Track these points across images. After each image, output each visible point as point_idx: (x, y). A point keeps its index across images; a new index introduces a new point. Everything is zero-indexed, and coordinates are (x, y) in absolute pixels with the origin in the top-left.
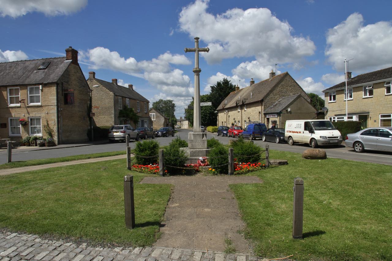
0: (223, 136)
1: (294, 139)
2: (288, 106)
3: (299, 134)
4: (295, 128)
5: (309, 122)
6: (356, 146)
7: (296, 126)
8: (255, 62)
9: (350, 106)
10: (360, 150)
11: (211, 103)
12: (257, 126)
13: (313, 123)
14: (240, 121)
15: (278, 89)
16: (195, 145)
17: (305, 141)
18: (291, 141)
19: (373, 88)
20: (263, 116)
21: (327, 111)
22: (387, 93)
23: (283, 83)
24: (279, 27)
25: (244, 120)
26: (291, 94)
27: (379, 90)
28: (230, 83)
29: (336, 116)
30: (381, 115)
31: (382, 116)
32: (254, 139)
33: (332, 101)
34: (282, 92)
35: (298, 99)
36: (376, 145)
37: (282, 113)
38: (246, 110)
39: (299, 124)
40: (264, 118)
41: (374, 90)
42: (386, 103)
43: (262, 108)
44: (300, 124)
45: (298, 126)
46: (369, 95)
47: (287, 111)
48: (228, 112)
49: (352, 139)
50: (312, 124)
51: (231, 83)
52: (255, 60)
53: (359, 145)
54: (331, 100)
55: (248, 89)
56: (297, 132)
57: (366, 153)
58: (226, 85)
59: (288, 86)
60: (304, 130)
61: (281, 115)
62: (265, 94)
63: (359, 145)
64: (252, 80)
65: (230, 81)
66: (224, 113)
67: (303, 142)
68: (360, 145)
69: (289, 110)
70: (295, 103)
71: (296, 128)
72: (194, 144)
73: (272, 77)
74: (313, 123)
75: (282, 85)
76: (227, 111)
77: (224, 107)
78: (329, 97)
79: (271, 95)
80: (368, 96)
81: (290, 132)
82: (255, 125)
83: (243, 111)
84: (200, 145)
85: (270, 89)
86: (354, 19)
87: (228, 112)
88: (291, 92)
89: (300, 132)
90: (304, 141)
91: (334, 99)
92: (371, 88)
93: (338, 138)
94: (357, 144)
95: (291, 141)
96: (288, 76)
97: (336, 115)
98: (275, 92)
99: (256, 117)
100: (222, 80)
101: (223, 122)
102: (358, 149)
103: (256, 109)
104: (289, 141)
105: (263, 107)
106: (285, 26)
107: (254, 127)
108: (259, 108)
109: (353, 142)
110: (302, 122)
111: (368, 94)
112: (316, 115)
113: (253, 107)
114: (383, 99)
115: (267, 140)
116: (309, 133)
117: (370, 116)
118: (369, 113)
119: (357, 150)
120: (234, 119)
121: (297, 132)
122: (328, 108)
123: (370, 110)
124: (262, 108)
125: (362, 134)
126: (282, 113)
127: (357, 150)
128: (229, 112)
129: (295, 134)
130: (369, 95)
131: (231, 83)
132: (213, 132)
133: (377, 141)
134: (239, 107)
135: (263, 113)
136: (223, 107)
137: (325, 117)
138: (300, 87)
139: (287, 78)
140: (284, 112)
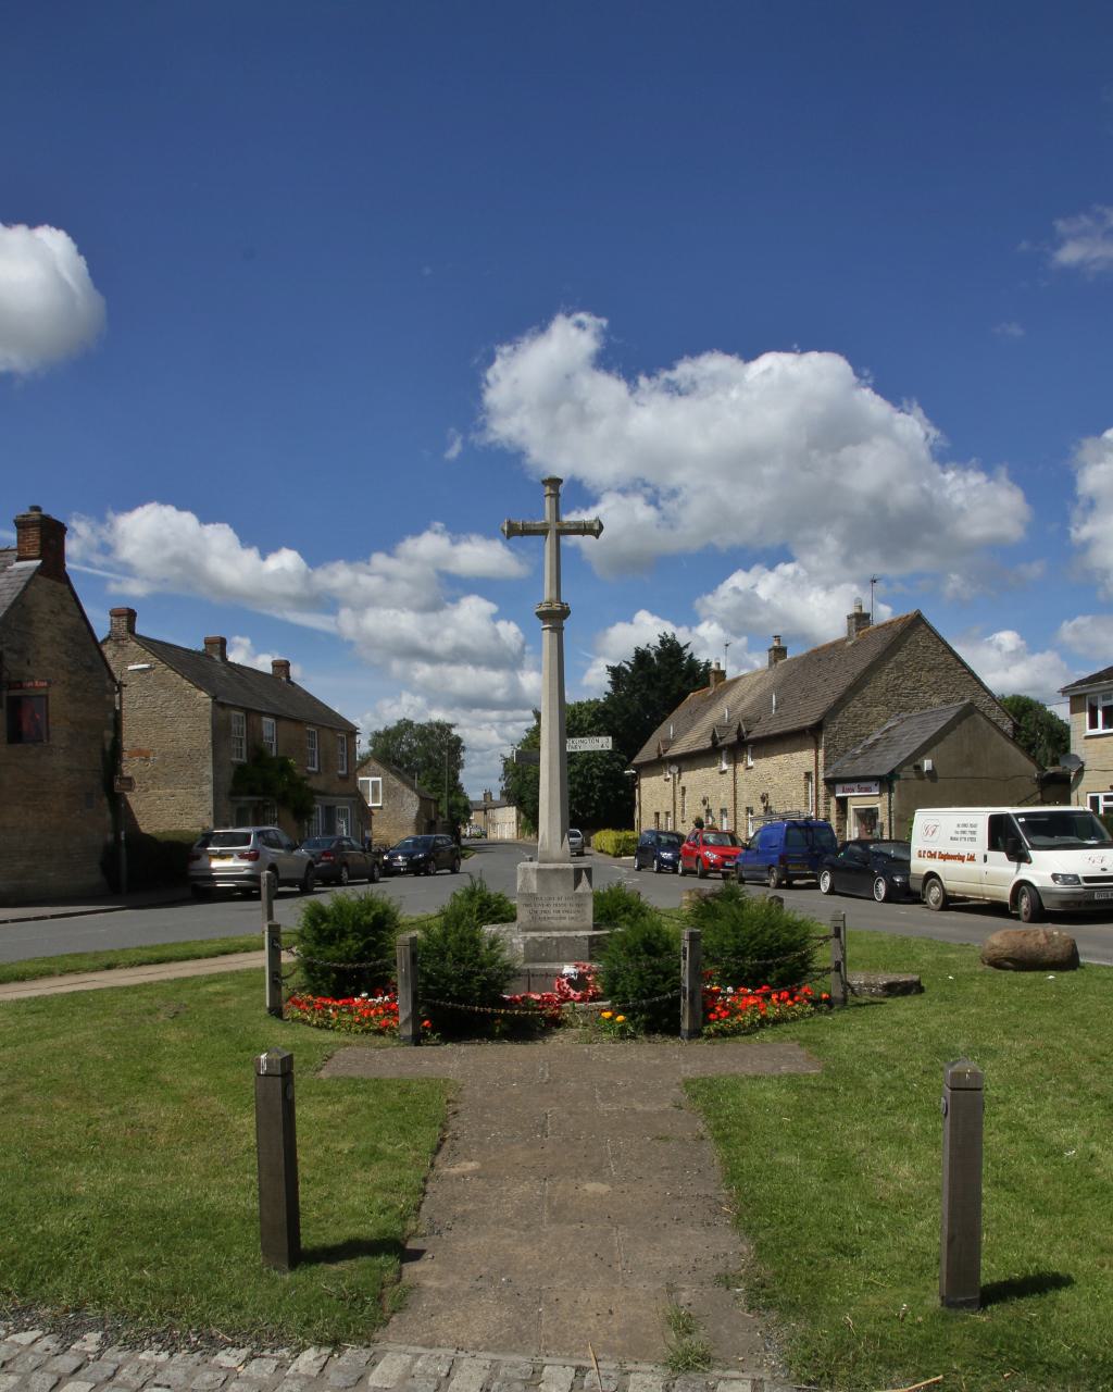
0: (659, 871)
1: (949, 885)
2: (924, 750)
3: (967, 865)
5: (1008, 815)
7: (957, 832)
8: (788, 569)
11: (610, 738)
12: (797, 833)
13: (1022, 820)
14: (730, 812)
15: (883, 679)
16: (543, 915)
17: (991, 893)
18: (935, 893)
20: (822, 789)
21: (1081, 772)
23: (901, 656)
24: (886, 430)
25: (744, 806)
26: (935, 700)
28: (687, 652)
32: (784, 882)
35: (964, 722)
37: (898, 777)
38: (751, 763)
39: (965, 825)
40: (827, 797)
43: (817, 757)
45: (964, 832)
47: (918, 768)
48: (680, 772)
50: (1021, 824)
51: (691, 655)
52: (789, 559)
54: (1093, 724)
55: (760, 681)
56: (961, 858)
58: (672, 660)
59: (921, 669)
60: (989, 849)
61: (895, 785)
62: (831, 700)
64: (776, 644)
65: (686, 646)
66: (662, 777)
67: (983, 895)
69: (927, 764)
70: (953, 735)
71: (955, 839)
73: (858, 630)
74: (1022, 820)
75: (899, 666)
76: (674, 769)
77: (665, 751)
78: (1087, 714)
79: (855, 706)
81: (932, 855)
82: (788, 828)
83: (741, 767)
84: (567, 915)
85: (849, 680)
87: (680, 772)
88: (936, 692)
89: (972, 858)
90: (986, 892)
95: (935, 893)
96: (922, 627)
98: (867, 691)
99: (794, 794)
100: (656, 642)
101: (657, 814)
104: (930, 891)
105: (821, 753)
106: (912, 426)
107: (787, 835)
108: (804, 759)
110: (978, 818)
112: (1036, 788)
113: (779, 754)
116: (1010, 859)
120: (704, 802)
121: (961, 858)
122: (1082, 759)
124: (817, 757)
126: (898, 777)
128: (684, 774)
129: (950, 863)
131: (691, 655)
132: (620, 856)
134: (724, 753)
135: (821, 776)
136: (659, 750)
137: (1073, 796)
138: (971, 673)
139: (918, 636)
140: (908, 772)
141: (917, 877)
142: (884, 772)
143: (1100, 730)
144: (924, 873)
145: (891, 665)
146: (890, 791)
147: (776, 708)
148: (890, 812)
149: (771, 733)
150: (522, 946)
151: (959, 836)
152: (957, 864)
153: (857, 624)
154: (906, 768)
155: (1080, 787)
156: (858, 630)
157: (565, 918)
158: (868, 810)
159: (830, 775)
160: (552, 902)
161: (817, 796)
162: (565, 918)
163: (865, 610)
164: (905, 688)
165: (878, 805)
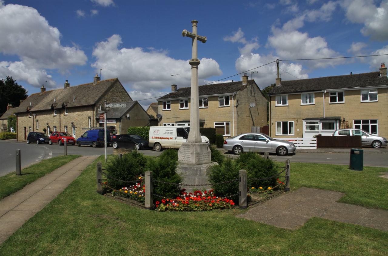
0: (39, 143)
1: (163, 145)
5: (183, 128)
6: (236, 149)
7: (166, 132)
8: (18, 63)
12: (101, 132)
13: (186, 129)
14: (32, 127)
15: (110, 94)
16: (201, 159)
18: (158, 147)
20: (95, 121)
21: (161, 118)
23: (113, 89)
24: (48, 32)
25: (64, 125)
26: (120, 100)
28: (15, 82)
29: (176, 123)
31: (216, 124)
32: (110, 145)
33: (167, 109)
34: (113, 98)
35: (136, 106)
36: (254, 148)
37: (122, 119)
38: (66, 114)
39: (169, 131)
40: (96, 123)
41: (209, 103)
42: (220, 113)
43: (93, 113)
44: (171, 131)
45: (168, 132)
46: (204, 106)
47: (126, 116)
48: (36, 116)
49: (232, 143)
50: (186, 130)
51: (17, 83)
52: (19, 60)
53: (238, 148)
54: (165, 108)
55: (62, 92)
56: (168, 139)
58: (11, 84)
60: (178, 136)
61: (121, 120)
62: (97, 98)
63: (238, 148)
64: (66, 82)
65: (15, 81)
66: (28, 117)
67: (175, 147)
68: (239, 148)
69: (128, 116)
70: (133, 109)
73: (97, 81)
74: (186, 129)
75: (113, 91)
76: (34, 115)
77: (30, 110)
78: (163, 106)
80: (203, 107)
82: (99, 131)
83: (62, 115)
85: (102, 94)
86: (115, 40)
87: (36, 116)
88: (121, 98)
89: (171, 138)
90: (176, 147)
91: (169, 107)
92: (207, 100)
93: (209, 143)
94: (236, 148)
95: (158, 147)
96: (118, 82)
97: (176, 122)
98: (106, 97)
99: (84, 122)
100: (5, 79)
101: (25, 128)
102: (238, 152)
103: (84, 114)
104: (156, 146)
105: (95, 112)
106: (55, 31)
107: (99, 134)
108: (89, 113)
109: (232, 146)
110: (174, 129)
111: (203, 105)
112: (149, 122)
113: (78, 111)
116: (184, 138)
118: (204, 121)
120: (47, 124)
121: (168, 139)
122: (162, 115)
123: (205, 118)
124: (93, 113)
125: (241, 138)
126: (122, 119)
127: (236, 153)
128: (37, 116)
129: (163, 140)
130: (204, 106)
131: (17, 83)
132: (5, 139)
133: (254, 144)
134: (55, 111)
135: (95, 118)
136: (27, 109)
137: (159, 124)
138: (128, 94)
139: (117, 84)
141: (151, 143)
142: (119, 117)
143: (167, 109)
144: (154, 142)
145: (111, 91)
146: (120, 122)
147: (75, 99)
148: (120, 127)
149: (76, 106)
150: (205, 170)
151: (166, 133)
152: (167, 140)
153: (97, 79)
154: (124, 116)
155: (161, 122)
156: (97, 81)
157: (205, 160)
158: (111, 127)
159: (97, 118)
160: (203, 155)
161: (90, 123)
162: (205, 160)
163: (98, 76)
164: (114, 97)
165: (115, 125)
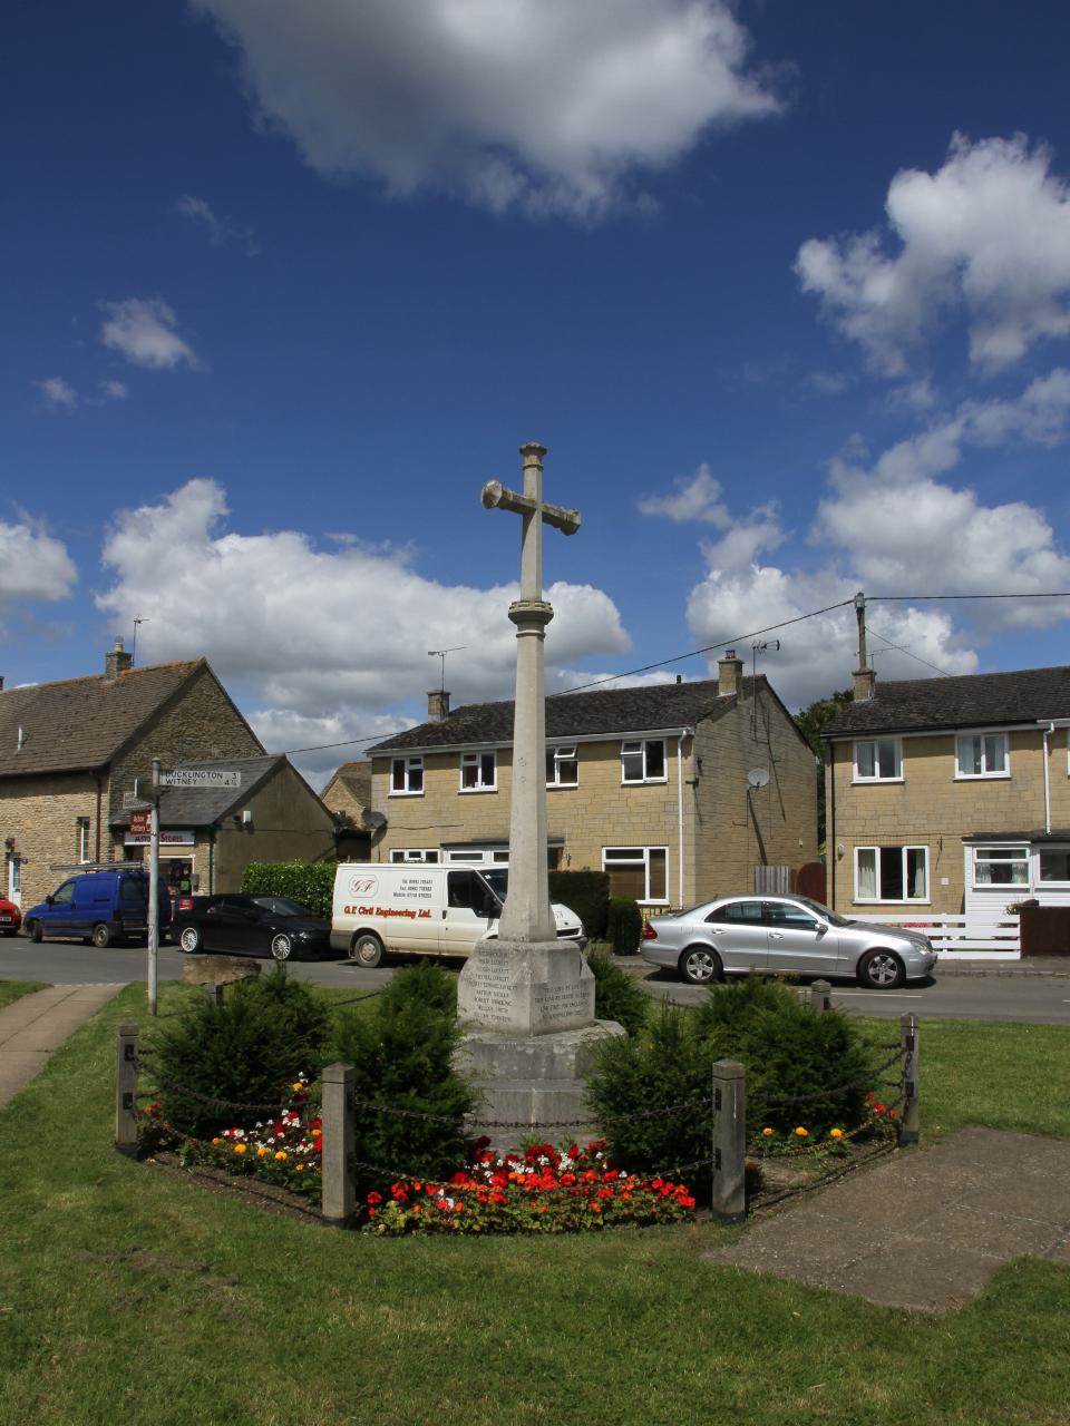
1: (389, 941)
2: (244, 801)
3: (419, 922)
4: (395, 895)
5: (473, 873)
6: (692, 962)
9: (484, 814)
10: (704, 974)
11: (239, 775)
12: (131, 884)
13: (488, 877)
15: (170, 724)
17: (451, 948)
18: (369, 949)
19: (576, 756)
20: (106, 837)
21: (383, 829)
22: (627, 777)
23: (187, 703)
26: (215, 751)
27: (598, 765)
29: (445, 849)
30: (608, 852)
31: (610, 854)
32: (168, 937)
33: (406, 791)
34: (184, 742)
35: (279, 775)
36: (768, 956)
39: (415, 882)
40: (111, 846)
41: (581, 767)
42: (628, 810)
44: (424, 882)
45: (414, 888)
46: (562, 781)
47: (238, 819)
49: (675, 937)
53: (700, 957)
54: (399, 784)
56: (412, 915)
57: (859, 989)
59: (204, 718)
60: (451, 904)
61: (218, 835)
62: (119, 742)
63: (700, 957)
68: (707, 957)
69: (246, 816)
70: (268, 788)
71: (400, 895)
72: (551, 1003)
73: (120, 669)
74: (488, 877)
75: (185, 711)
78: (392, 776)
79: (141, 750)
80: (557, 783)
81: (366, 911)
82: (123, 879)
84: (573, 1009)
85: (137, 723)
86: (199, 500)
89: (426, 914)
90: (444, 948)
91: (416, 782)
92: (573, 755)
93: (580, 934)
94: (694, 956)
95: (369, 949)
96: (207, 676)
97: (446, 846)
98: (155, 735)
99: (59, 840)
102: (700, 973)
103: (61, 806)
105: (106, 798)
107: (121, 888)
108: (83, 802)
109: (678, 948)
110: (436, 877)
111: (557, 775)
112: (332, 843)
114: (616, 797)
115: (206, 948)
117: (566, 852)
118: (562, 841)
119: (694, 976)
121: (412, 915)
122: (387, 817)
123: (567, 830)
125: (717, 917)
127: (694, 976)
129: (391, 920)
130: (562, 781)
133: (768, 942)
135: (105, 823)
137: (374, 851)
139: (203, 684)
140: (229, 823)
141: (342, 934)
142: (207, 820)
143: (406, 791)
144: (355, 929)
145: (177, 711)
146: (212, 841)
147: (23, 744)
148: (211, 864)
149: (29, 770)
150: (572, 1057)
151: (406, 892)
152: (406, 921)
153: (119, 663)
154: (227, 819)
155: (381, 843)
156: (120, 669)
157: (570, 1014)
158: (172, 860)
159: (117, 822)
160: (561, 994)
161: (86, 845)
162: (570, 1014)
163: (126, 651)
164: (189, 736)
165: (192, 856)
